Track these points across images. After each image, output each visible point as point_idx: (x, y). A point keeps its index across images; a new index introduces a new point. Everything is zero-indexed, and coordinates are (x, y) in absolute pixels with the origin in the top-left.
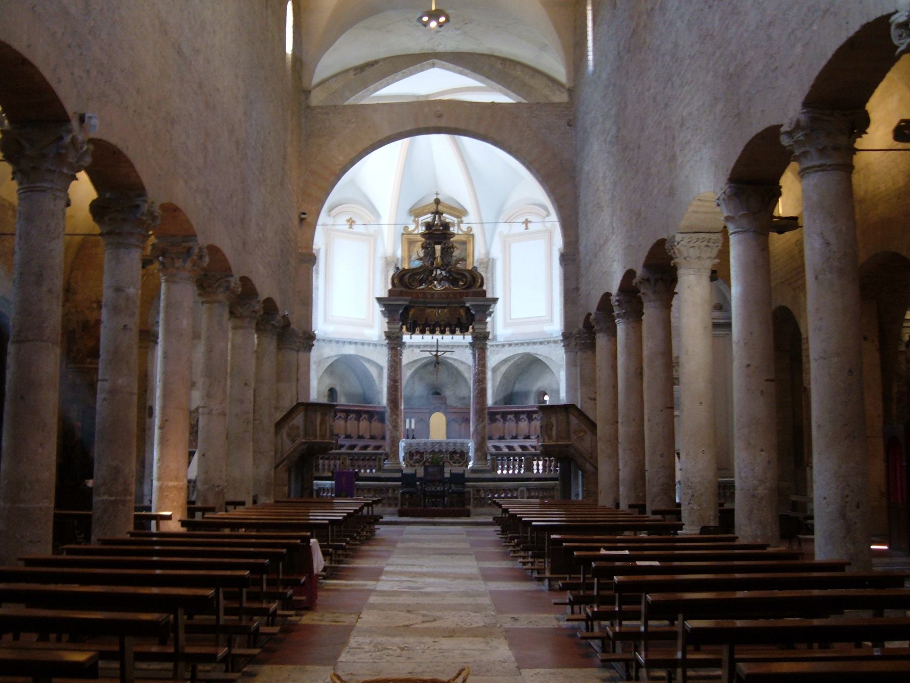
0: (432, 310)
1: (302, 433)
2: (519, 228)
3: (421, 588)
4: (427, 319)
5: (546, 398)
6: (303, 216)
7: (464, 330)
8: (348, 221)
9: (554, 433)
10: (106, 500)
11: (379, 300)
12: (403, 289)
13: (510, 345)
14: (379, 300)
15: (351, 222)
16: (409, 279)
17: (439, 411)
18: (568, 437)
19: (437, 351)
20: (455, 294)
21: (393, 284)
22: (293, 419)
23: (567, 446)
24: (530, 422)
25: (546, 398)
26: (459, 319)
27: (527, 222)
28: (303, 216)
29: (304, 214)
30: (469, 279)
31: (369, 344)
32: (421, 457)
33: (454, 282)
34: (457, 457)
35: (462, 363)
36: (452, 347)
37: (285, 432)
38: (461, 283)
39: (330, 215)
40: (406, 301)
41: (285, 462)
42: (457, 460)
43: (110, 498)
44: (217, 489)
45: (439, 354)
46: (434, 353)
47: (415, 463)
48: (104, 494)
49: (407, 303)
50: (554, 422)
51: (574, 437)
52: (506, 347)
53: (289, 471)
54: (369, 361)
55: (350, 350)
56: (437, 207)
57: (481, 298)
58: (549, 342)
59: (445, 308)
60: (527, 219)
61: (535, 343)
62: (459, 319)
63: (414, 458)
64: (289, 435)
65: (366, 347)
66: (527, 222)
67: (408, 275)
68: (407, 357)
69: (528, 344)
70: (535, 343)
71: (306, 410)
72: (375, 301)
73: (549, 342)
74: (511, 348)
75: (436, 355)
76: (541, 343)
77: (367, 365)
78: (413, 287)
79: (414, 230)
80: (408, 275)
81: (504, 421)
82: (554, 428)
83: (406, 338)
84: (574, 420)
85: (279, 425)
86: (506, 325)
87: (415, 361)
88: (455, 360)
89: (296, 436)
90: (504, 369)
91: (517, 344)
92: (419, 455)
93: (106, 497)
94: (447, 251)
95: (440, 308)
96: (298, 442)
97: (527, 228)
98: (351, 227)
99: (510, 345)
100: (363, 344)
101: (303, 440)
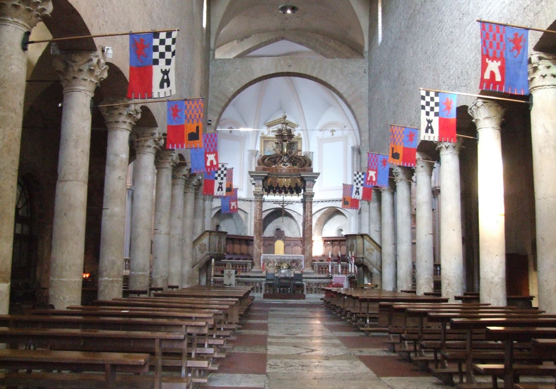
0: (281, 179)
1: (207, 248)
2: (328, 134)
3: (295, 335)
4: (278, 183)
7: (298, 192)
10: (107, 280)
13: (322, 201)
17: (280, 239)
19: (283, 204)
20: (294, 170)
21: (259, 164)
22: (202, 240)
23: (363, 258)
26: (296, 184)
27: (333, 131)
28: (210, 122)
30: (303, 162)
33: (294, 164)
36: (291, 203)
37: (197, 247)
40: (266, 173)
41: (198, 265)
42: (294, 267)
43: (109, 279)
44: (164, 278)
45: (284, 205)
46: (282, 205)
48: (106, 276)
49: (266, 175)
51: (366, 253)
52: (320, 203)
59: (288, 178)
62: (296, 184)
63: (269, 265)
64: (200, 249)
66: (333, 131)
67: (268, 158)
71: (210, 235)
74: (323, 203)
75: (282, 206)
78: (269, 166)
79: (267, 135)
83: (266, 197)
85: (195, 242)
89: (204, 250)
91: (326, 201)
93: (107, 278)
94: (291, 145)
95: (286, 178)
96: (205, 253)
97: (333, 135)
99: (322, 201)
101: (208, 253)
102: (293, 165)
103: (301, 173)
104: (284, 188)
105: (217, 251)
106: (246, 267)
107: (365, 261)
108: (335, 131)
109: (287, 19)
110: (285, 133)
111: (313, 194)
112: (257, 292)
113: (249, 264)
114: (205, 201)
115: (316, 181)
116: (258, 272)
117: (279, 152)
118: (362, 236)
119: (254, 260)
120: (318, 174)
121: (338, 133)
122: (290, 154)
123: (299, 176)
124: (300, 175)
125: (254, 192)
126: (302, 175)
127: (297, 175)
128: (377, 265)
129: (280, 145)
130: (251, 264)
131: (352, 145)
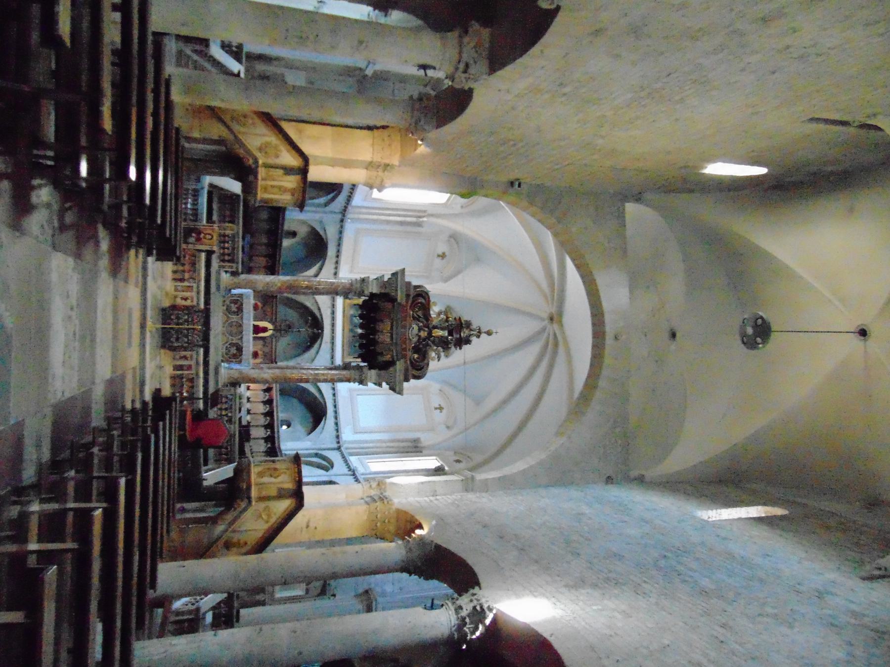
0: (390, 326)
1: (271, 161)
2: (436, 401)
5: (284, 427)
6: (517, 183)
8: (444, 253)
9: (266, 479)
11: (403, 271)
12: (411, 297)
13: (334, 395)
14: (403, 271)
15: (443, 256)
16: (421, 303)
18: (261, 499)
21: (416, 287)
24: (262, 414)
25: (284, 427)
27: (440, 408)
29: (519, 185)
31: (336, 268)
32: (234, 312)
33: (416, 350)
34: (233, 350)
35: (317, 353)
38: (416, 356)
39: (451, 237)
40: (402, 299)
42: (229, 351)
47: (228, 306)
50: (280, 479)
51: (262, 505)
52: (331, 391)
53: (220, 142)
54: (321, 269)
55: (331, 252)
56: (485, 333)
57: (402, 378)
58: (337, 430)
60: (443, 408)
61: (336, 418)
63: (232, 305)
64: (267, 145)
65: (333, 266)
66: (440, 408)
68: (323, 301)
69: (336, 412)
70: (336, 418)
72: (403, 267)
73: (337, 430)
74: (331, 396)
76: (336, 424)
77: (318, 265)
80: (423, 301)
81: (264, 390)
82: (272, 480)
84: (285, 505)
86: (350, 391)
87: (319, 309)
88: (320, 345)
90: (312, 389)
91: (335, 402)
92: (236, 310)
94: (444, 344)
96: (258, 154)
97: (436, 409)
98: (439, 256)
99: (334, 395)
100: (337, 262)
101: (260, 162)
102: (413, 348)
103: (402, 361)
104: (375, 331)
105: (264, 183)
106: (229, 261)
107: (243, 505)
108: (441, 412)
109: (646, 335)
110: (464, 333)
111: (365, 383)
112: (175, 272)
113: (234, 265)
114: (367, 168)
115: (380, 385)
116: (218, 280)
117: (434, 323)
118: (298, 496)
119: (243, 276)
120: (400, 393)
121: (439, 417)
122: (433, 342)
123: (395, 358)
124: (398, 360)
125: (369, 277)
126: (398, 363)
127: (397, 356)
128: (234, 531)
129: (443, 325)
130: (234, 270)
131: (422, 440)
